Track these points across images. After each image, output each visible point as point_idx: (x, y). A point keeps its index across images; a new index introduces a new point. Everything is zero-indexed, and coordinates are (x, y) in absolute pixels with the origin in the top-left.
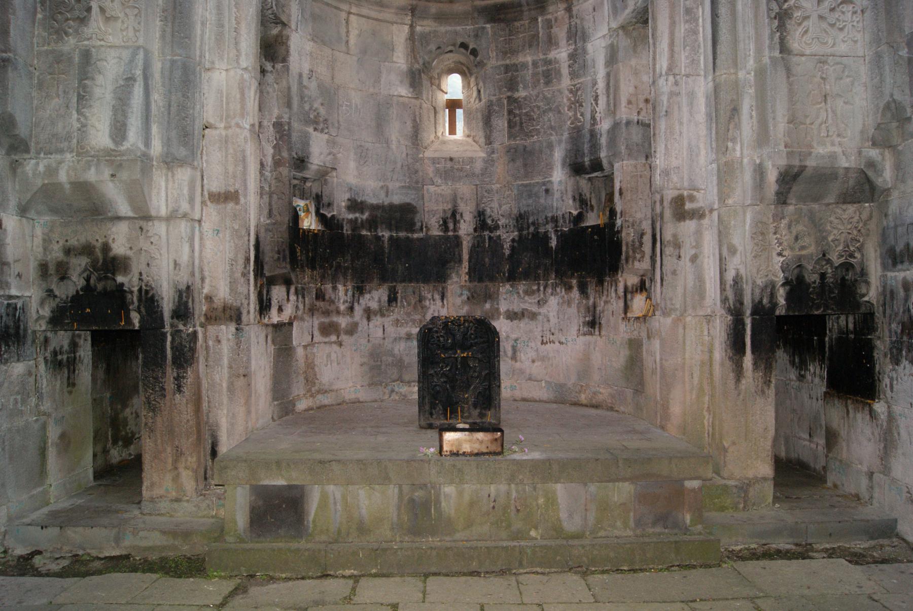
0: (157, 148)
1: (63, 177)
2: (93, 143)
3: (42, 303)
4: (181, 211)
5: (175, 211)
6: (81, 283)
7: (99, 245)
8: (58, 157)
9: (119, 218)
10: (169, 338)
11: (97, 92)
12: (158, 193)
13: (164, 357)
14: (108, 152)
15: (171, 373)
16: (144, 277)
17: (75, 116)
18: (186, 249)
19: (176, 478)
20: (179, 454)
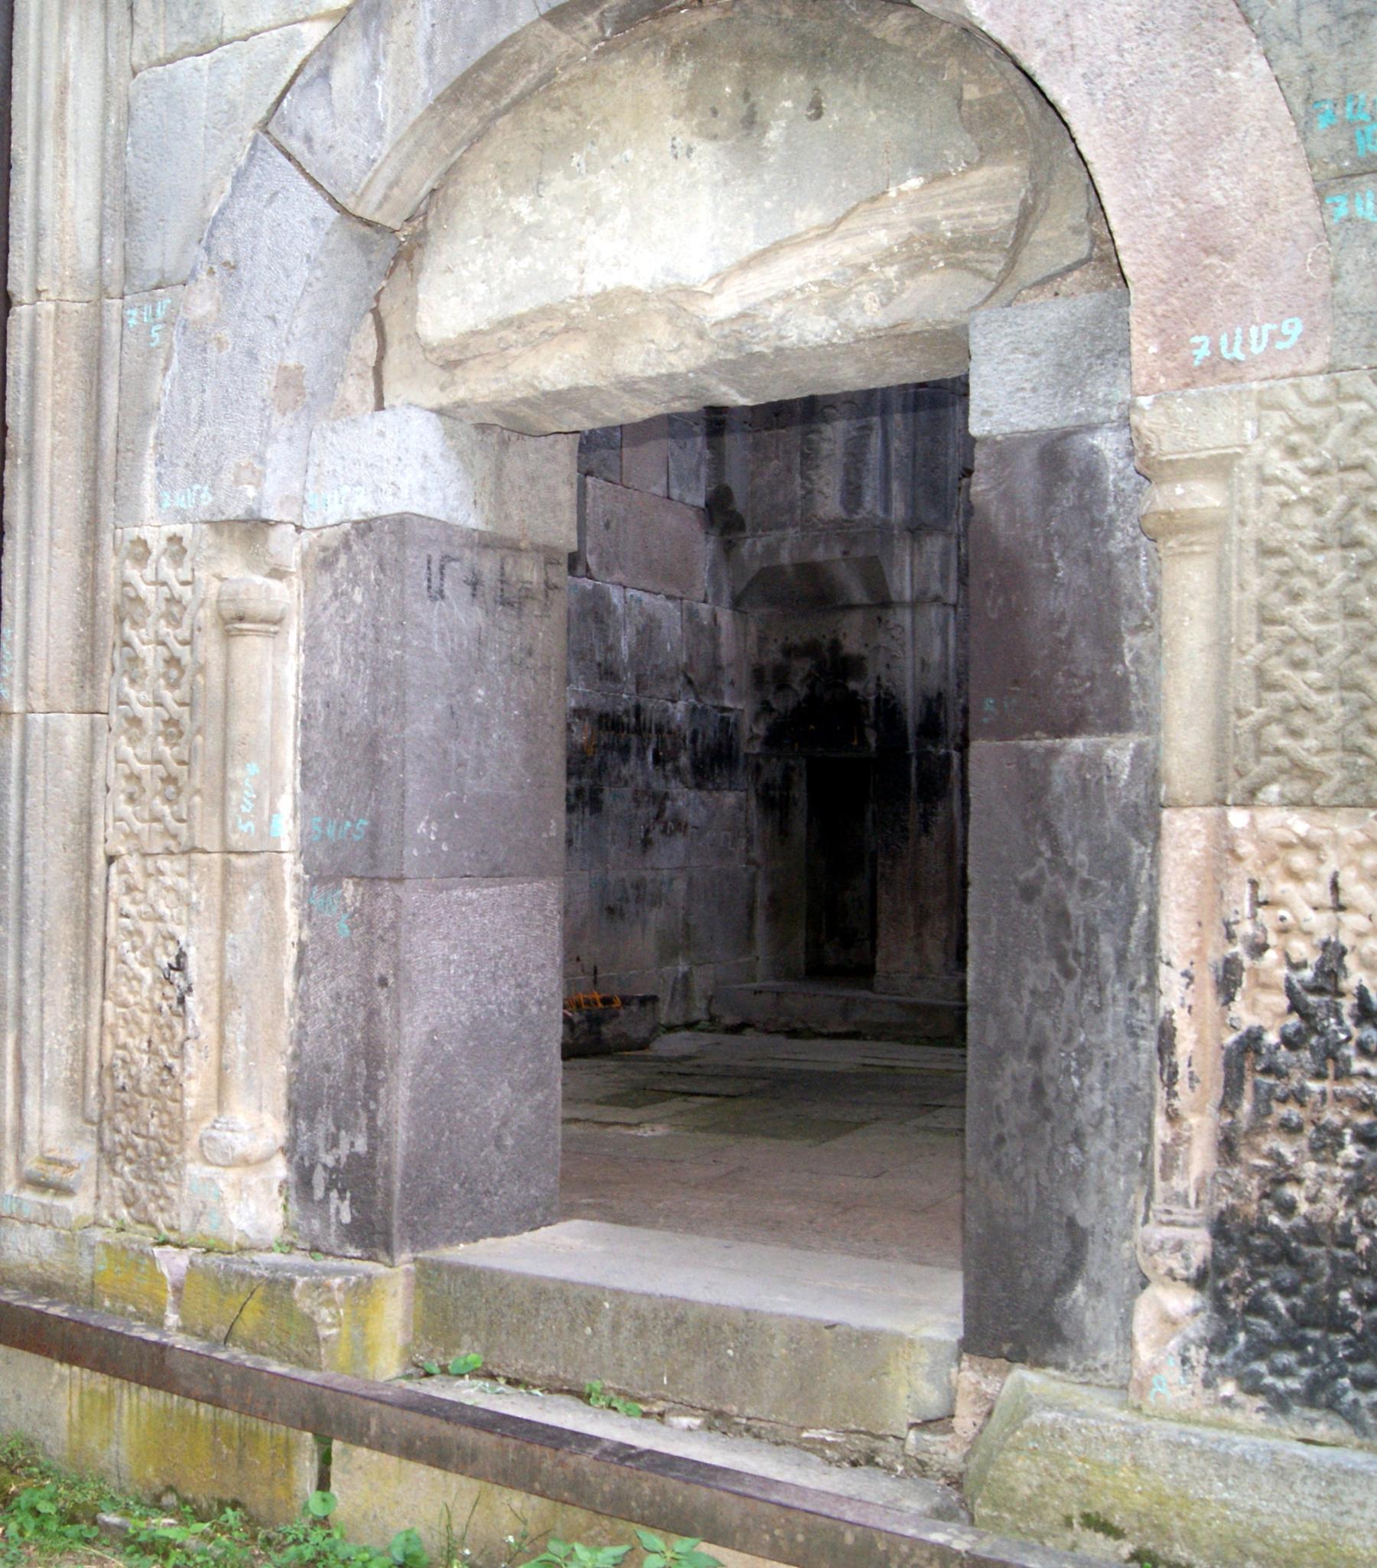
0: (899, 510)
1: (785, 558)
2: (821, 513)
3: (756, 718)
4: (930, 595)
5: (924, 593)
6: (803, 692)
7: (826, 643)
8: (777, 534)
9: (850, 607)
10: (914, 763)
11: (825, 447)
12: (902, 571)
13: (908, 786)
14: (838, 524)
15: (915, 809)
16: (884, 682)
17: (798, 480)
18: (937, 642)
19: (919, 949)
20: (923, 917)
